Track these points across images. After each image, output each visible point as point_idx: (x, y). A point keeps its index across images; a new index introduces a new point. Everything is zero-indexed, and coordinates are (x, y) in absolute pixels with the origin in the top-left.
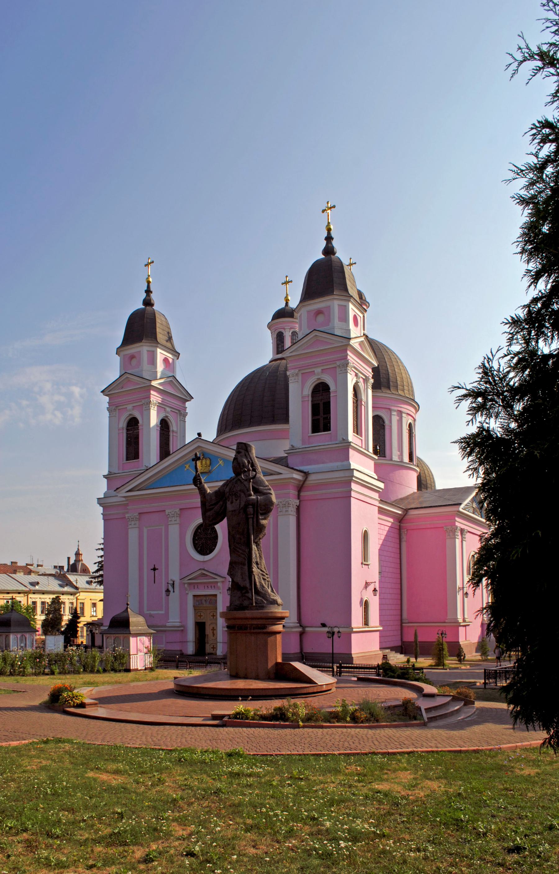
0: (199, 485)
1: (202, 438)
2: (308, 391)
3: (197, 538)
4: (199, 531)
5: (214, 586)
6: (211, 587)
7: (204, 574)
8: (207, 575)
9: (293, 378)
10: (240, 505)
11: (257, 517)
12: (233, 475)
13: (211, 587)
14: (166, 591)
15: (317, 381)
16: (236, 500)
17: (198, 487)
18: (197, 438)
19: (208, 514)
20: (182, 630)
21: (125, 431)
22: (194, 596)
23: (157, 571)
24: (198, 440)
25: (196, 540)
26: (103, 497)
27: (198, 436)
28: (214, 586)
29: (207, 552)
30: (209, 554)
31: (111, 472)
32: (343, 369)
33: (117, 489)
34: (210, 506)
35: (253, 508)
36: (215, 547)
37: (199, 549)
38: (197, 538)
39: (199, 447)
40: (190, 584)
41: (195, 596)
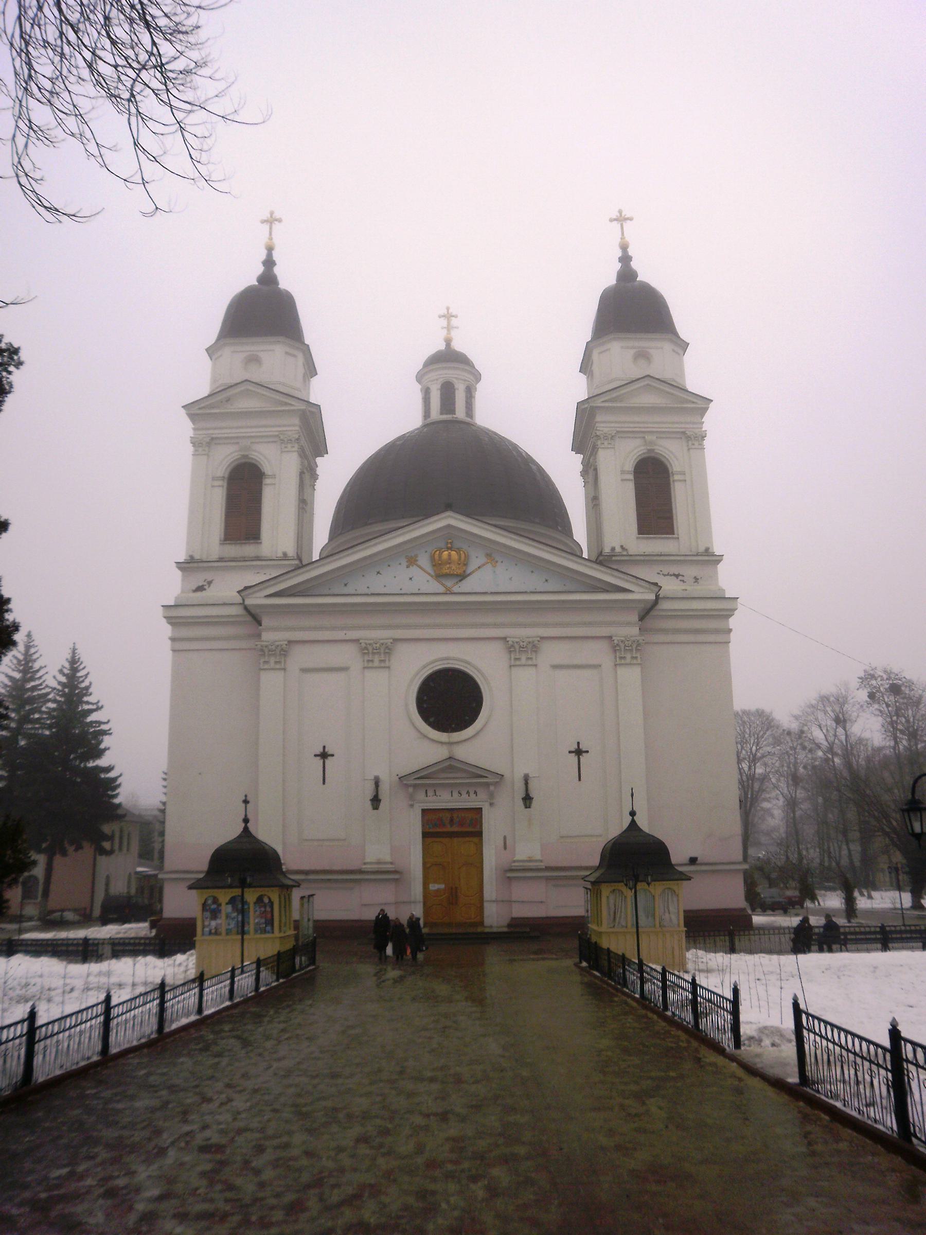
2: (630, 466)
5: (475, 793)
6: (468, 793)
9: (606, 443)
13: (468, 793)
14: (370, 800)
15: (644, 453)
20: (397, 879)
21: (225, 485)
22: (424, 811)
23: (329, 761)
26: (173, 604)
28: (475, 793)
31: (192, 557)
32: (696, 443)
33: (246, 588)
37: (432, 720)
39: (449, 526)
40: (415, 786)
41: (424, 811)
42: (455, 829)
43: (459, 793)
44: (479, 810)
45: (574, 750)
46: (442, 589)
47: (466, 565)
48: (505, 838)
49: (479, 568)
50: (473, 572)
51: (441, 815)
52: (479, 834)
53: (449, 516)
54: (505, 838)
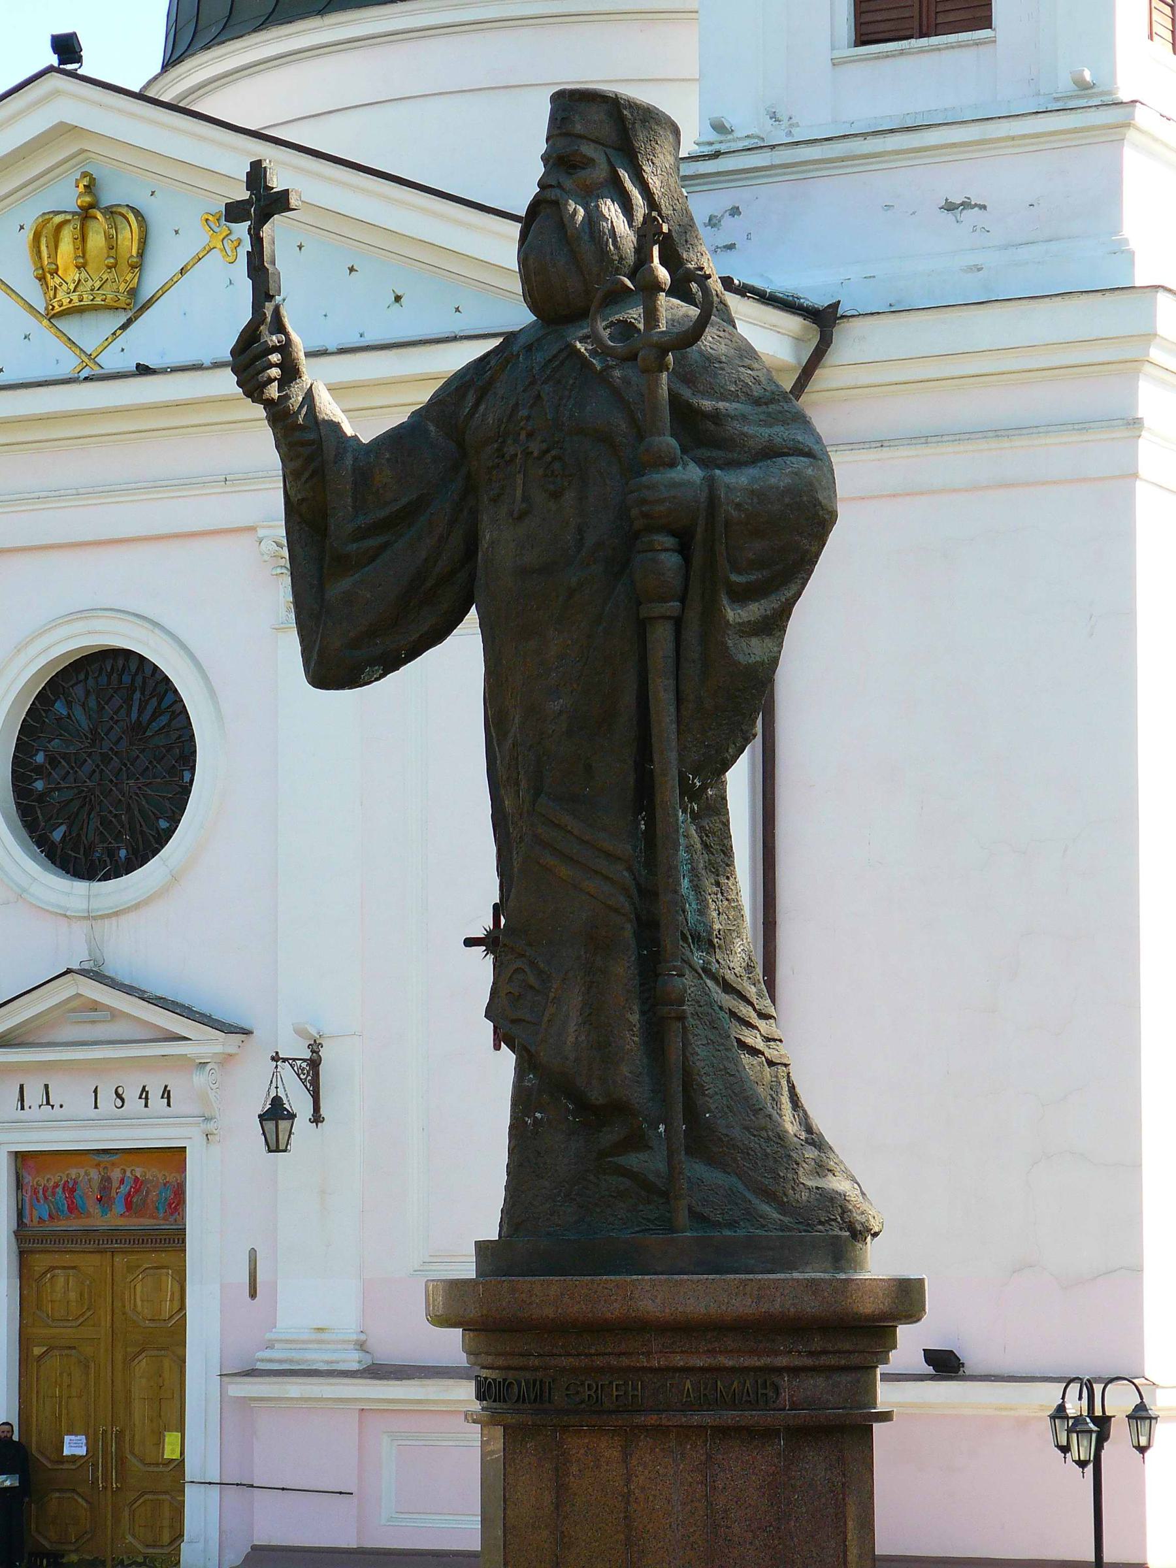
0: (273, 391)
1: (87, 68)
3: (40, 758)
4: (60, 707)
5: (166, 1094)
6: (144, 1094)
7: (95, 1006)
8: (114, 1015)
10: (580, 530)
11: (711, 614)
12: (520, 316)
16: (556, 495)
17: (269, 404)
18: (50, 69)
19: (338, 588)
24: (56, 81)
25: (39, 770)
27: (54, 60)
29: (112, 853)
30: (129, 867)
34: (362, 534)
35: (684, 550)
36: (175, 821)
37: (57, 835)
38: (40, 758)
39: (63, 131)
42: (114, 1218)
43: (119, 1096)
44: (175, 1156)
45: (480, 934)
46: (69, 363)
47: (138, 264)
48: (253, 1254)
49: (182, 271)
50: (164, 290)
51: (73, 1173)
52: (175, 1240)
53: (56, 93)
54: (253, 1254)
